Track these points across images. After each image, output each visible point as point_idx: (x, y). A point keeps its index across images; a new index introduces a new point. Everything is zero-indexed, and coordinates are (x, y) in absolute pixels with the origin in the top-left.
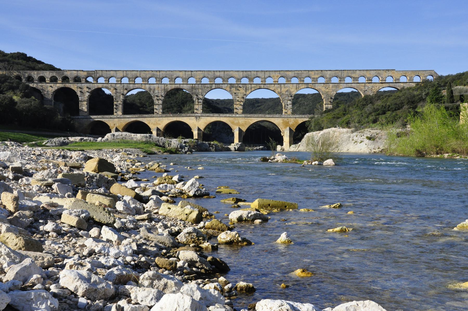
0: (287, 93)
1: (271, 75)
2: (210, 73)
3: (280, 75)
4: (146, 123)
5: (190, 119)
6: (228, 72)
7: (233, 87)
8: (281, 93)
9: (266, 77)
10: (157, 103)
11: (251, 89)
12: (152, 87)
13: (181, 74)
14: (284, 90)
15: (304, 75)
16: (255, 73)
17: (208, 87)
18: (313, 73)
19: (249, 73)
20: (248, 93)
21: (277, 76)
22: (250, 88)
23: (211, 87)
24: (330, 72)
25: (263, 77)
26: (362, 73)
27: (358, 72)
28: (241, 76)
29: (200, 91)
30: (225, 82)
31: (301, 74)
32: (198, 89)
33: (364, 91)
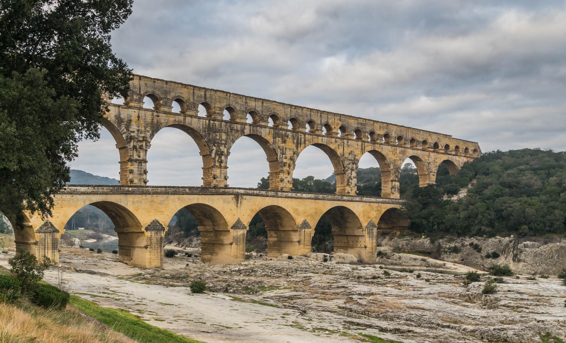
0: (351, 157)
2: (239, 101)
3: (340, 124)
4: (130, 208)
6: (268, 104)
8: (343, 155)
9: (323, 122)
10: (136, 157)
12: (125, 114)
13: (185, 94)
14: (347, 151)
15: (368, 129)
16: (308, 113)
17: (237, 131)
18: (377, 125)
19: (299, 111)
21: (338, 124)
22: (303, 140)
25: (319, 122)
28: (289, 115)
29: (224, 137)
30: (263, 124)
31: (365, 125)
32: (220, 131)
33: (429, 163)
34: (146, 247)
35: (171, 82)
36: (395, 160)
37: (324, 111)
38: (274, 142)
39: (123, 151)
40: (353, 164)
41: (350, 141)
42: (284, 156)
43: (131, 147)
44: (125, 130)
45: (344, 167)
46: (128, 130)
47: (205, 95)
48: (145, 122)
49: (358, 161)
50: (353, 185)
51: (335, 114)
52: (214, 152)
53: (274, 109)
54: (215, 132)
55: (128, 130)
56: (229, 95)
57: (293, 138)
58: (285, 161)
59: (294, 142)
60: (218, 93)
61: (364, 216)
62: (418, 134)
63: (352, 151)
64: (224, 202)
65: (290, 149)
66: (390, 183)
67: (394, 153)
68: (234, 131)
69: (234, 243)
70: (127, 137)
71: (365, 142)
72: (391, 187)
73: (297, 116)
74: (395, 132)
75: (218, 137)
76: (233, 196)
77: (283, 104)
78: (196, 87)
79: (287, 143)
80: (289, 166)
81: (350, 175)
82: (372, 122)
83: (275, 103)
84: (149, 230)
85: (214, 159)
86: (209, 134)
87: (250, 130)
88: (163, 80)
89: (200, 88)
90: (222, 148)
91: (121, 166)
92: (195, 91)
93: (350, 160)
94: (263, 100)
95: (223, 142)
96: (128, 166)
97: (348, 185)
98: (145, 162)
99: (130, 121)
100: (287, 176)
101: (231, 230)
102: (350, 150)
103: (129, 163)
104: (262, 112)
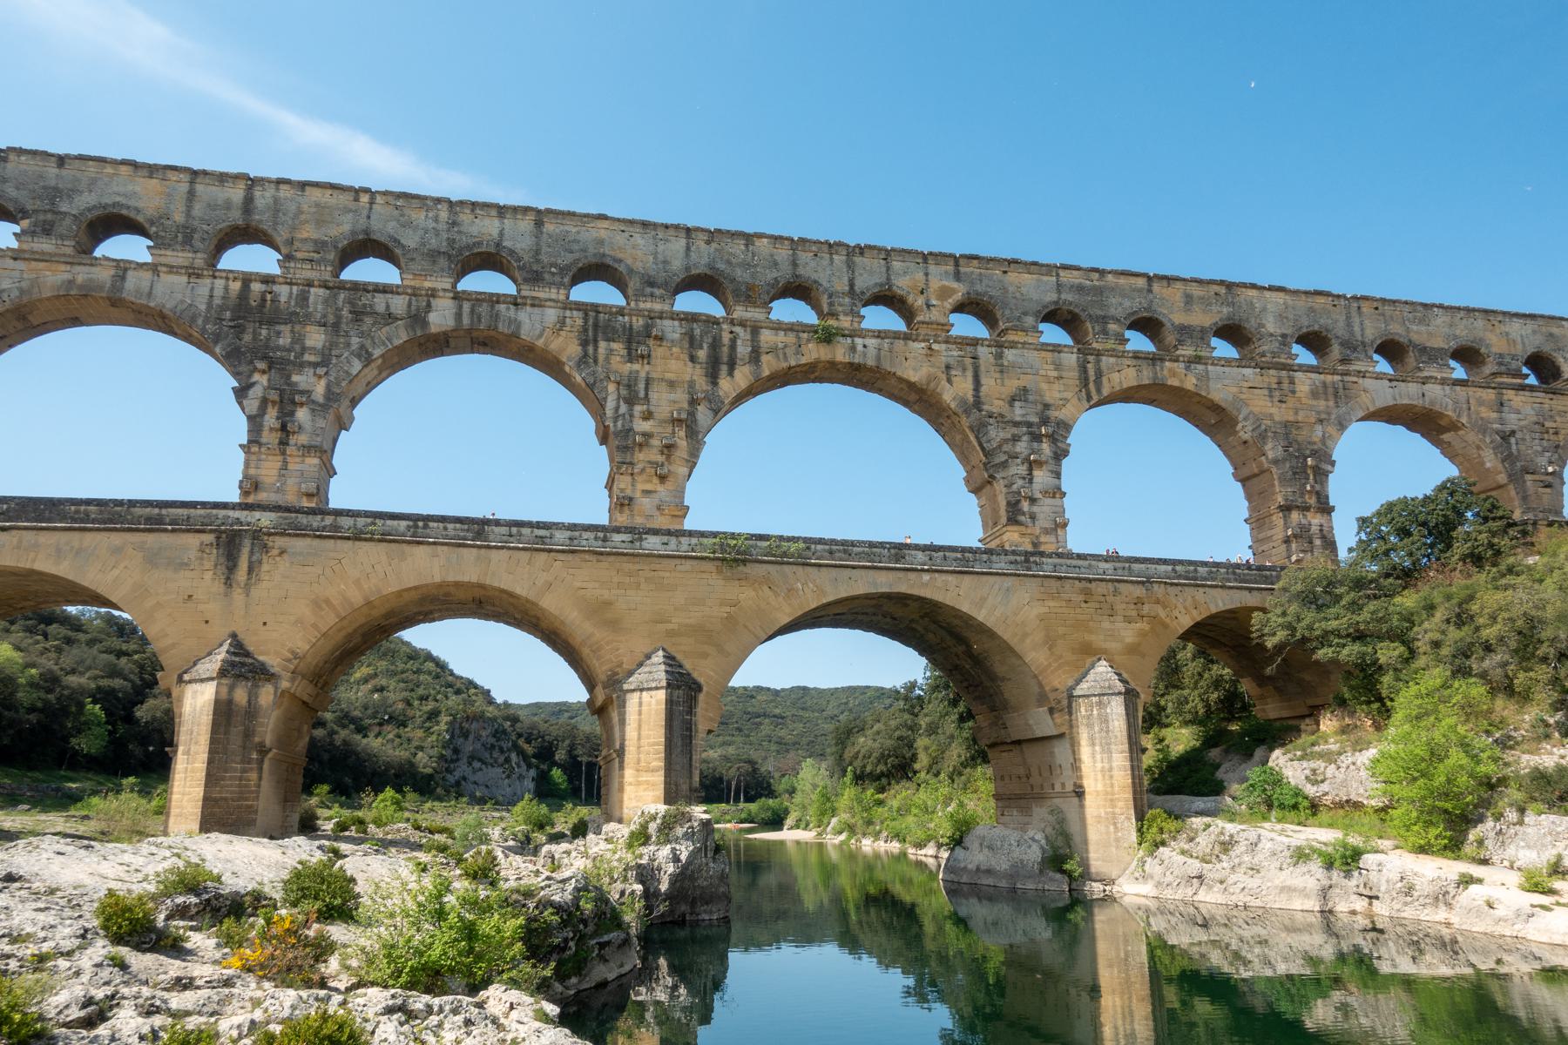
0: (1018, 412)
1: (903, 284)
2: (419, 217)
3: (960, 291)
5: (151, 559)
6: (571, 228)
7: (610, 334)
8: (978, 404)
9: (860, 284)
11: (755, 356)
13: (146, 198)
15: (1120, 306)
17: (390, 317)
18: (1176, 293)
20: (728, 386)
21: (944, 293)
22: (743, 350)
23: (417, 319)
24: (1280, 298)
26: (1464, 332)
27: (1441, 320)
28: (677, 264)
29: (316, 338)
31: (1099, 291)
32: (296, 317)
33: (1506, 437)
35: (81, 158)
36: (1286, 424)
37: (861, 250)
38: (583, 361)
40: (1037, 438)
41: (1010, 355)
42: (638, 409)
45: (986, 453)
47: (248, 201)
49: (1066, 427)
50: (1043, 522)
51: (925, 257)
52: (256, 392)
53: (601, 242)
54: (271, 322)
56: (365, 198)
57: (692, 342)
58: (641, 426)
59: (693, 359)
60: (315, 195)
61: (1050, 642)
62: (1421, 321)
63: (1025, 390)
64: (151, 559)
65: (672, 384)
66: (1278, 519)
67: (1281, 391)
68: (368, 320)
71: (1098, 354)
73: (721, 266)
74: (1281, 317)
75: (285, 340)
76: (209, 538)
77: (645, 225)
78: (205, 173)
79: (653, 361)
80: (669, 448)
81: (1020, 482)
82: (1141, 282)
83: (605, 224)
86: (239, 330)
87: (459, 316)
88: (45, 154)
89: (223, 178)
90: (301, 379)
92: (199, 188)
93: (1016, 424)
94: (540, 217)
95: (312, 358)
97: (1013, 521)
100: (655, 484)
102: (1012, 385)
104: (538, 252)
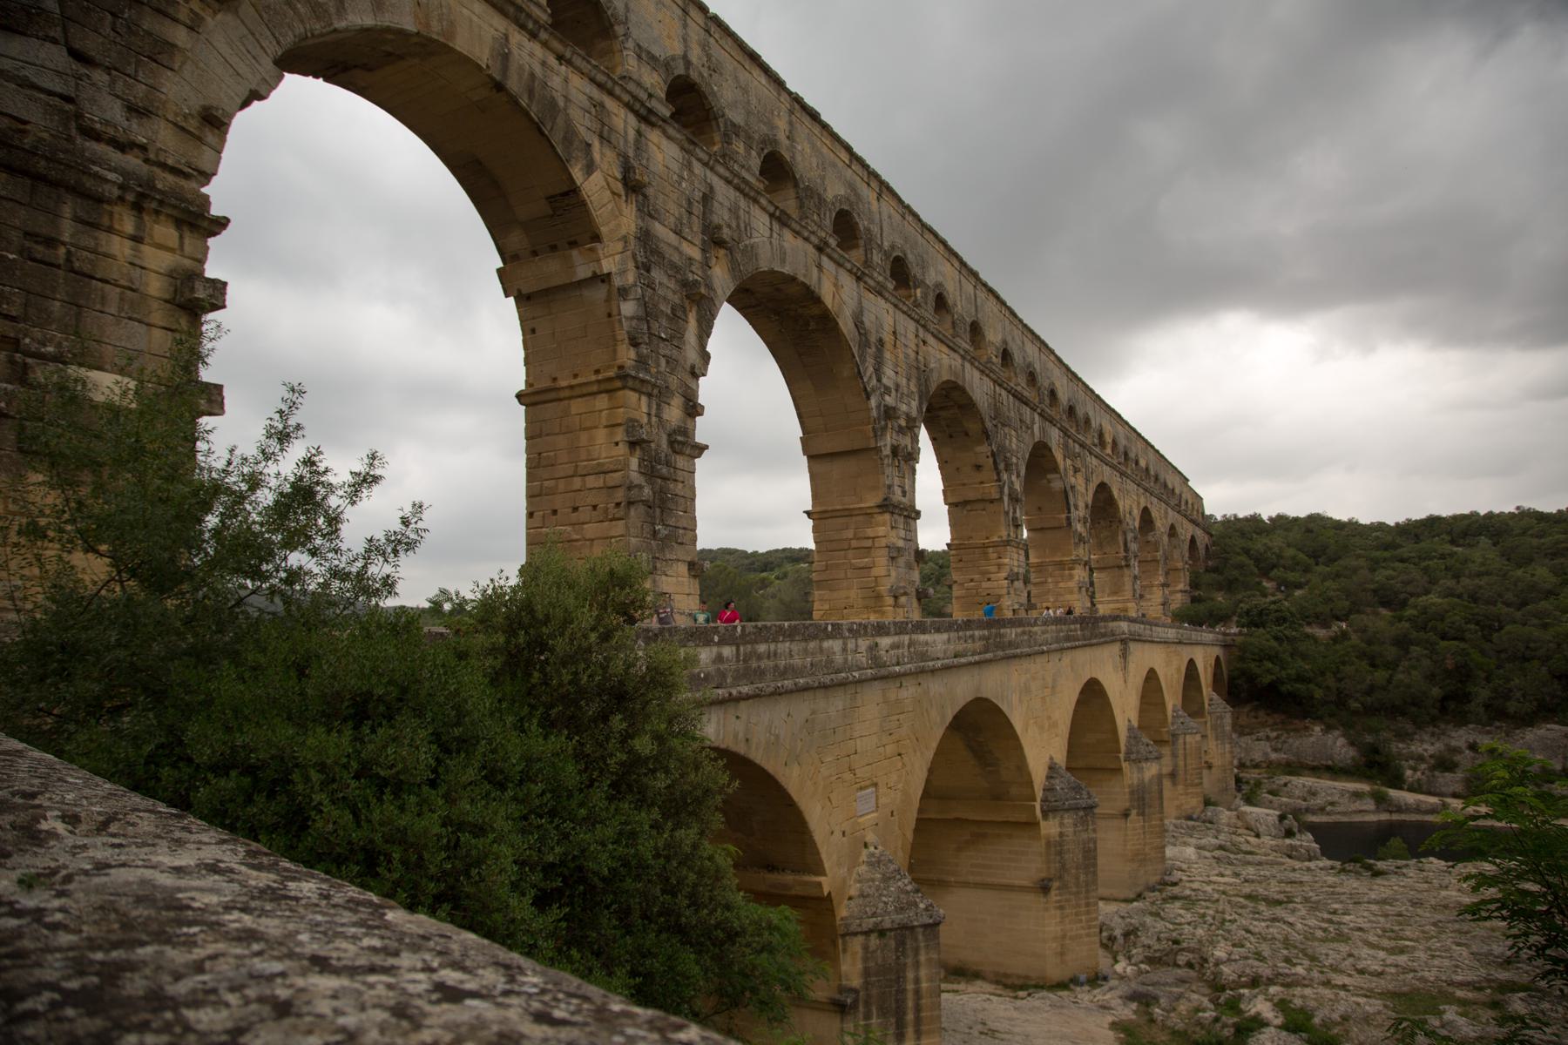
34: (1044, 888)
39: (836, 469)
43: (887, 451)
44: (874, 381)
45: (1126, 550)
46: (879, 380)
48: (907, 356)
52: (1006, 490)
55: (879, 380)
69: (1134, 812)
70: (878, 407)
72: (1160, 600)
84: (1055, 810)
85: (1007, 513)
91: (815, 530)
96: (881, 530)
98: (918, 514)
99: (881, 342)
101: (1125, 765)
103: (887, 516)
